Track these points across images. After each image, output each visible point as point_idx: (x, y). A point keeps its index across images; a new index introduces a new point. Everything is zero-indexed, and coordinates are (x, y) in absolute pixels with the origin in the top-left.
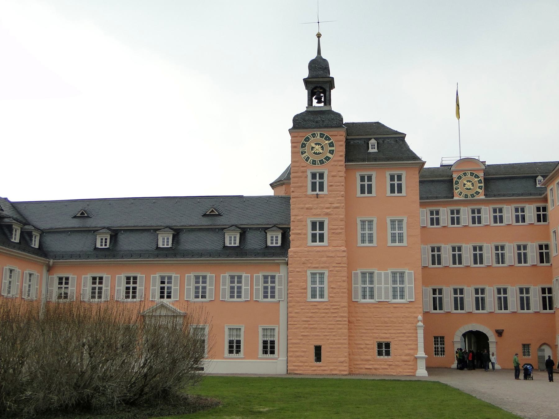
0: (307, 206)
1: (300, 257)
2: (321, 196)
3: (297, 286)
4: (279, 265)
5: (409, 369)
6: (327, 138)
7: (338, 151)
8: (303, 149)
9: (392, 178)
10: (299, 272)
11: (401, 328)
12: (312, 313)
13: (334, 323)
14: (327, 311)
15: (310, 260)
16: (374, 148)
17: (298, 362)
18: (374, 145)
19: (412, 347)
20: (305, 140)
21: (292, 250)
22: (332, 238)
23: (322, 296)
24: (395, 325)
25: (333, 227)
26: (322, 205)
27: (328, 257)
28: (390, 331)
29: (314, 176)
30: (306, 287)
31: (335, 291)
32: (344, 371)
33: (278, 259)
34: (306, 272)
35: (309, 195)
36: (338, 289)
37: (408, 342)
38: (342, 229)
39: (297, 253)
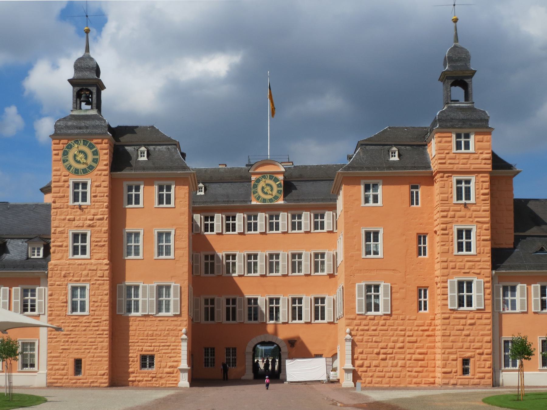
0: (68, 217)
1: (61, 270)
2: (82, 207)
3: (58, 299)
4: (40, 278)
5: (172, 381)
6: (91, 147)
7: (102, 160)
8: (65, 157)
9: (161, 188)
10: (59, 285)
11: (166, 341)
12: (72, 326)
13: (95, 336)
14: (87, 324)
15: (70, 273)
16: (144, 156)
17: (58, 375)
18: (144, 153)
19: (176, 359)
20: (67, 147)
21: (52, 262)
22: (95, 251)
23: (83, 309)
24: (159, 338)
25: (96, 239)
26: (84, 217)
27: (90, 270)
28: (153, 344)
29: (76, 185)
30: (65, 300)
31: (96, 304)
32: (105, 383)
33: (36, 272)
34: (67, 285)
35: (71, 206)
36: (100, 302)
37: (172, 355)
38: (105, 241)
39: (57, 266)
